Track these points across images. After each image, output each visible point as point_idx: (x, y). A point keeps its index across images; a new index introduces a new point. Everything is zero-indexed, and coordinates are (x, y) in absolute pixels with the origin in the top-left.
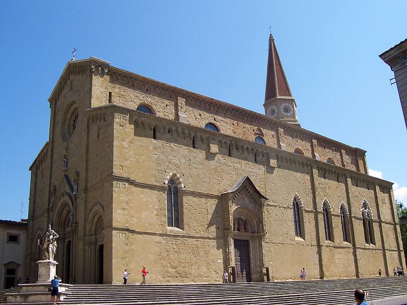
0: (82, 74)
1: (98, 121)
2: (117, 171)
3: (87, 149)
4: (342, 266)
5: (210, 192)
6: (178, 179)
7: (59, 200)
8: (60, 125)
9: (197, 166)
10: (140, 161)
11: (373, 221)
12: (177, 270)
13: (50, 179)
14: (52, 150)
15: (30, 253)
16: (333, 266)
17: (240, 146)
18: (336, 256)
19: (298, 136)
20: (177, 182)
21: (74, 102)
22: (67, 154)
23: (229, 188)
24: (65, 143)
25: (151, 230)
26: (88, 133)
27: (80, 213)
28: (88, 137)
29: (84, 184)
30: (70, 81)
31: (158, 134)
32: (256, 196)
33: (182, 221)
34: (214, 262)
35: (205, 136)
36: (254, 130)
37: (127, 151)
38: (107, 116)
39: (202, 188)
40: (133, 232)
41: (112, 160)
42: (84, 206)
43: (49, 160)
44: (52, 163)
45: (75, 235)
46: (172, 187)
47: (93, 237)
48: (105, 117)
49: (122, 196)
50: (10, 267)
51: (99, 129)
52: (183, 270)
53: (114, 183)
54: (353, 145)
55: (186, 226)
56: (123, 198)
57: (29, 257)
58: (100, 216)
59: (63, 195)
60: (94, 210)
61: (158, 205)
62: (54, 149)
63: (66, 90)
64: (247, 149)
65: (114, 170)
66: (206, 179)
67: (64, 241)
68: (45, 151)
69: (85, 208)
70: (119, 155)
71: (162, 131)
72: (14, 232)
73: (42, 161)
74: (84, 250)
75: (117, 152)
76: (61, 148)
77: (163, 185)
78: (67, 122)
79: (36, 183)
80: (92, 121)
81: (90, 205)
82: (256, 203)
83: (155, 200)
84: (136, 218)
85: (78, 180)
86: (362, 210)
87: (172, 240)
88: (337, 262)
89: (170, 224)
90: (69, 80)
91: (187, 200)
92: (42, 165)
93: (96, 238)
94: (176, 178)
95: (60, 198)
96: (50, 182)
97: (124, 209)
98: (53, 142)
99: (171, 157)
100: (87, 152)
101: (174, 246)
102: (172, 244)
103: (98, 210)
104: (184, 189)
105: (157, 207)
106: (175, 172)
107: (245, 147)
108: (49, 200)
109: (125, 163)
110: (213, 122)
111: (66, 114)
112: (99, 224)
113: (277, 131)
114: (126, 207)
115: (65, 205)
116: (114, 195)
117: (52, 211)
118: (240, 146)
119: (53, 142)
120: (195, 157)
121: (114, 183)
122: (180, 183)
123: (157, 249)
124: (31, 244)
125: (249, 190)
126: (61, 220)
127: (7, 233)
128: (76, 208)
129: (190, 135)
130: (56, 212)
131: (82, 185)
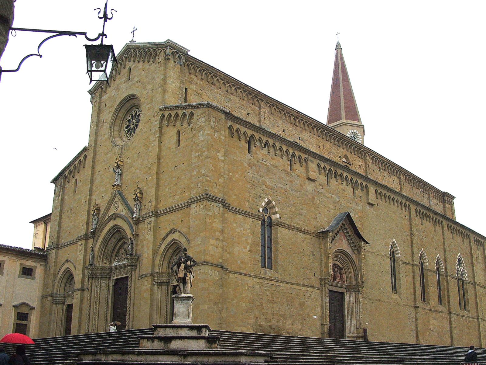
1: (178, 124)
4: (436, 334)
5: (306, 228)
7: (107, 223)
8: (107, 125)
10: (234, 179)
11: (467, 282)
13: (90, 195)
14: (94, 157)
15: (50, 292)
16: (428, 333)
17: (339, 174)
18: (432, 322)
19: (386, 169)
22: (122, 164)
26: (160, 137)
27: (145, 242)
28: (160, 143)
29: (153, 203)
31: (254, 148)
32: (355, 239)
33: (276, 262)
34: (309, 316)
35: (304, 156)
36: (340, 157)
37: (222, 164)
38: (195, 117)
42: (152, 232)
44: (93, 174)
45: (135, 270)
46: (266, 219)
49: (215, 222)
51: (179, 133)
52: (276, 324)
54: (443, 189)
58: (178, 248)
59: (114, 217)
60: (169, 239)
61: (252, 239)
62: (98, 156)
64: (346, 178)
66: (302, 211)
67: (110, 278)
68: (82, 158)
69: (155, 236)
71: (258, 144)
72: (29, 263)
73: (74, 173)
74: (152, 290)
77: (257, 213)
79: (62, 200)
81: (163, 233)
83: (248, 231)
84: (228, 253)
86: (456, 267)
90: (124, 68)
94: (271, 205)
95: (109, 221)
96: (90, 200)
97: (217, 239)
98: (95, 147)
99: (266, 179)
100: (159, 163)
102: (265, 290)
105: (250, 241)
106: (270, 198)
108: (88, 223)
109: (220, 180)
110: (298, 141)
113: (365, 160)
114: (221, 238)
119: (95, 147)
123: (250, 295)
126: (106, 251)
128: (137, 235)
129: (287, 153)
130: (100, 240)
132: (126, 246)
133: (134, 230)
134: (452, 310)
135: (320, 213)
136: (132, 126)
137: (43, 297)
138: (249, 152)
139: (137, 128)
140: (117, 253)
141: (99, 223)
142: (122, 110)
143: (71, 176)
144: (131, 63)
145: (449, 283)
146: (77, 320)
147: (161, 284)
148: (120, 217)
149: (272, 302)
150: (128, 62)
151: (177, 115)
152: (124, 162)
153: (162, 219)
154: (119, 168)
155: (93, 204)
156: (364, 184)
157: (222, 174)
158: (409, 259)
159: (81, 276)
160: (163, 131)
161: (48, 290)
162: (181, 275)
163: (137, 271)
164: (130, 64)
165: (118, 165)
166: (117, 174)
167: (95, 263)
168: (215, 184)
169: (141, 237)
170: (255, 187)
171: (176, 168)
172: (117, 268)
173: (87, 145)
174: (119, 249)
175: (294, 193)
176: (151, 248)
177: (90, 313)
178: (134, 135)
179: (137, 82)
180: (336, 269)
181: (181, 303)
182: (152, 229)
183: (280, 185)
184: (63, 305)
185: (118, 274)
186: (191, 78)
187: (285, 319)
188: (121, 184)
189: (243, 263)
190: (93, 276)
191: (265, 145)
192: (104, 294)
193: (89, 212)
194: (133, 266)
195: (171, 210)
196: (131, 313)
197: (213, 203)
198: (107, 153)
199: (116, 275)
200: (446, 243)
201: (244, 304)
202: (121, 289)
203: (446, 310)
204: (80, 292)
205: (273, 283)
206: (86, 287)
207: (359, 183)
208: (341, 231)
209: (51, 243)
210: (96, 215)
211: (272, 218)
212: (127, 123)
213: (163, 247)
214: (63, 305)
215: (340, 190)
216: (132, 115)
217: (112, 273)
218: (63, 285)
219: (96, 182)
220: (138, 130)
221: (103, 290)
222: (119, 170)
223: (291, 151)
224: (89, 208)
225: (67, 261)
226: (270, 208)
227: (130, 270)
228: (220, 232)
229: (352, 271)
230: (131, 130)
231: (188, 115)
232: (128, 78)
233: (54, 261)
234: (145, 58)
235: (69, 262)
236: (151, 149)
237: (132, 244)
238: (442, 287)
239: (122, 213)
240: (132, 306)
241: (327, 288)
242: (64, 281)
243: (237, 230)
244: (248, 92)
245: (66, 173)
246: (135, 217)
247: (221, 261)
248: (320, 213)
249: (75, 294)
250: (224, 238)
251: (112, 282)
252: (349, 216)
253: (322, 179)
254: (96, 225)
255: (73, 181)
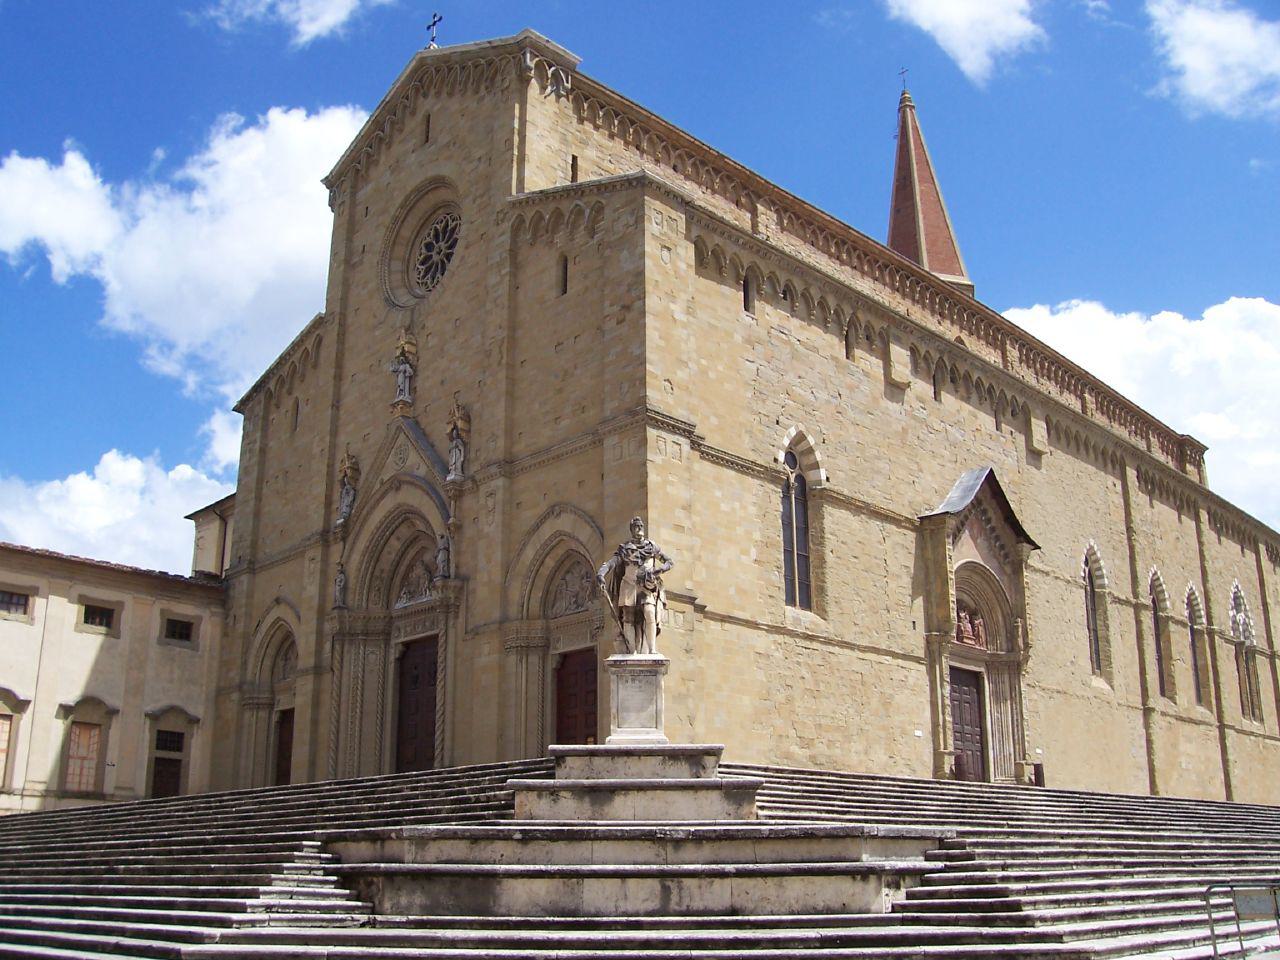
0: (478, 87)
1: (560, 238)
2: (657, 397)
3: (513, 327)
4: (1194, 777)
6: (811, 451)
8: (372, 259)
9: (858, 418)
10: (712, 375)
12: (814, 751)
13: (334, 433)
16: (1175, 775)
17: (962, 372)
18: (1184, 747)
20: (806, 461)
21: (439, 182)
23: (935, 499)
24: (399, 318)
25: (743, 609)
26: (514, 275)
29: (501, 443)
30: (420, 116)
32: (1007, 535)
33: (822, 590)
34: (904, 733)
35: (878, 325)
39: (872, 491)
40: (700, 609)
41: (642, 361)
42: (498, 517)
43: (326, 373)
44: (338, 377)
45: (457, 617)
46: (792, 480)
47: (539, 624)
48: (594, 220)
49: (672, 484)
50: (171, 725)
52: (827, 752)
53: (652, 433)
54: (1180, 428)
55: (832, 609)
56: (679, 492)
57: (235, 696)
58: (570, 553)
59: (396, 484)
60: (547, 531)
63: (404, 146)
64: (978, 385)
65: (650, 393)
66: (881, 465)
68: (309, 344)
69: (507, 527)
70: (662, 343)
71: (766, 288)
72: (184, 609)
73: (291, 383)
74: (502, 667)
75: (657, 334)
76: (377, 333)
77: (773, 465)
78: (400, 251)
79: (263, 451)
80: (535, 236)
81: (529, 516)
82: (1006, 556)
83: (752, 510)
84: (707, 566)
85: (469, 431)
86: (1231, 613)
87: (799, 650)
88: (1183, 766)
89: (790, 600)
90: (413, 113)
91: (834, 519)
92: (290, 393)
93: (548, 629)
94: (802, 447)
95: (382, 497)
96: (333, 447)
97: (679, 528)
98: (343, 315)
99: (790, 377)
101: (804, 672)
102: (799, 663)
103: (568, 529)
104: (826, 485)
105: (757, 536)
106: (802, 428)
107: (975, 377)
108: (328, 503)
109: (680, 374)
111: (399, 221)
112: (557, 581)
114: (687, 524)
115: (406, 515)
116: (653, 478)
117: (344, 539)
118: (962, 372)
120: (851, 388)
121: (652, 433)
122: (816, 466)
123: (761, 676)
124: (246, 652)
125: (991, 514)
126: (377, 573)
127: (163, 612)
128: (459, 527)
129: (838, 316)
130: (362, 543)
131: (490, 445)
132: (427, 557)
133: (452, 514)
134: (1227, 720)
135: (921, 471)
136: (436, 258)
137: (220, 693)
138: (747, 308)
139: (449, 261)
140: (406, 577)
141: (358, 501)
142: (409, 219)
143: (284, 390)
144: (431, 100)
145: (1218, 651)
146: (306, 748)
147: (525, 650)
148: (414, 482)
149: (815, 694)
150: (422, 99)
151: (558, 215)
152: (421, 345)
153: (524, 481)
154: (407, 361)
155: (341, 455)
156: (1021, 400)
157: (684, 358)
158: (1125, 593)
159: (313, 638)
160: (520, 258)
161: (232, 674)
162: (628, 600)
163: (461, 620)
164: (426, 105)
165: (403, 353)
166: (401, 376)
167: (350, 602)
168: (667, 383)
169: (469, 531)
170: (764, 397)
171: (559, 348)
172: (407, 614)
173: (324, 312)
174: (410, 568)
175: (858, 417)
176: (498, 556)
177: (338, 732)
178: (444, 280)
179: (447, 145)
180: (962, 615)
181: (633, 680)
182: (499, 508)
183: (823, 395)
184: (270, 714)
185: (408, 629)
186: (585, 132)
187: (848, 739)
188: (414, 400)
189: (741, 591)
190: (343, 636)
191: (784, 293)
192: (373, 681)
193: (330, 474)
194: (448, 606)
195: (547, 457)
196: (448, 728)
197: (664, 434)
198: (375, 328)
199: (403, 631)
200: (1206, 553)
201: (746, 700)
202: (417, 668)
203: (1213, 719)
204: (311, 678)
205: (815, 645)
206: (326, 662)
207: (1009, 397)
208: (972, 517)
209: (238, 559)
210: (349, 483)
211: (808, 480)
212: (424, 251)
213: (530, 553)
214: (270, 714)
215: (964, 414)
216: (436, 230)
217: (394, 628)
218: (268, 663)
219: (349, 401)
220: (450, 267)
221: (370, 672)
222: (408, 366)
223: (848, 310)
224: (331, 466)
225: (278, 601)
226: (802, 453)
227: (442, 617)
228: (684, 508)
229: (1000, 618)
230: (434, 268)
231: (588, 211)
232: (424, 137)
233: (244, 601)
234: (466, 83)
235: (282, 606)
236: (489, 306)
237: (447, 549)
238: (1200, 663)
239: (417, 473)
240: (449, 708)
241: (946, 663)
242: (271, 651)
243: (724, 507)
244: (724, 173)
245: (272, 385)
246: (453, 482)
247: (689, 585)
248: (921, 471)
249: (300, 682)
250: (693, 524)
251: (392, 651)
252: (991, 478)
253: (922, 388)
254: (351, 506)
255: (288, 403)
